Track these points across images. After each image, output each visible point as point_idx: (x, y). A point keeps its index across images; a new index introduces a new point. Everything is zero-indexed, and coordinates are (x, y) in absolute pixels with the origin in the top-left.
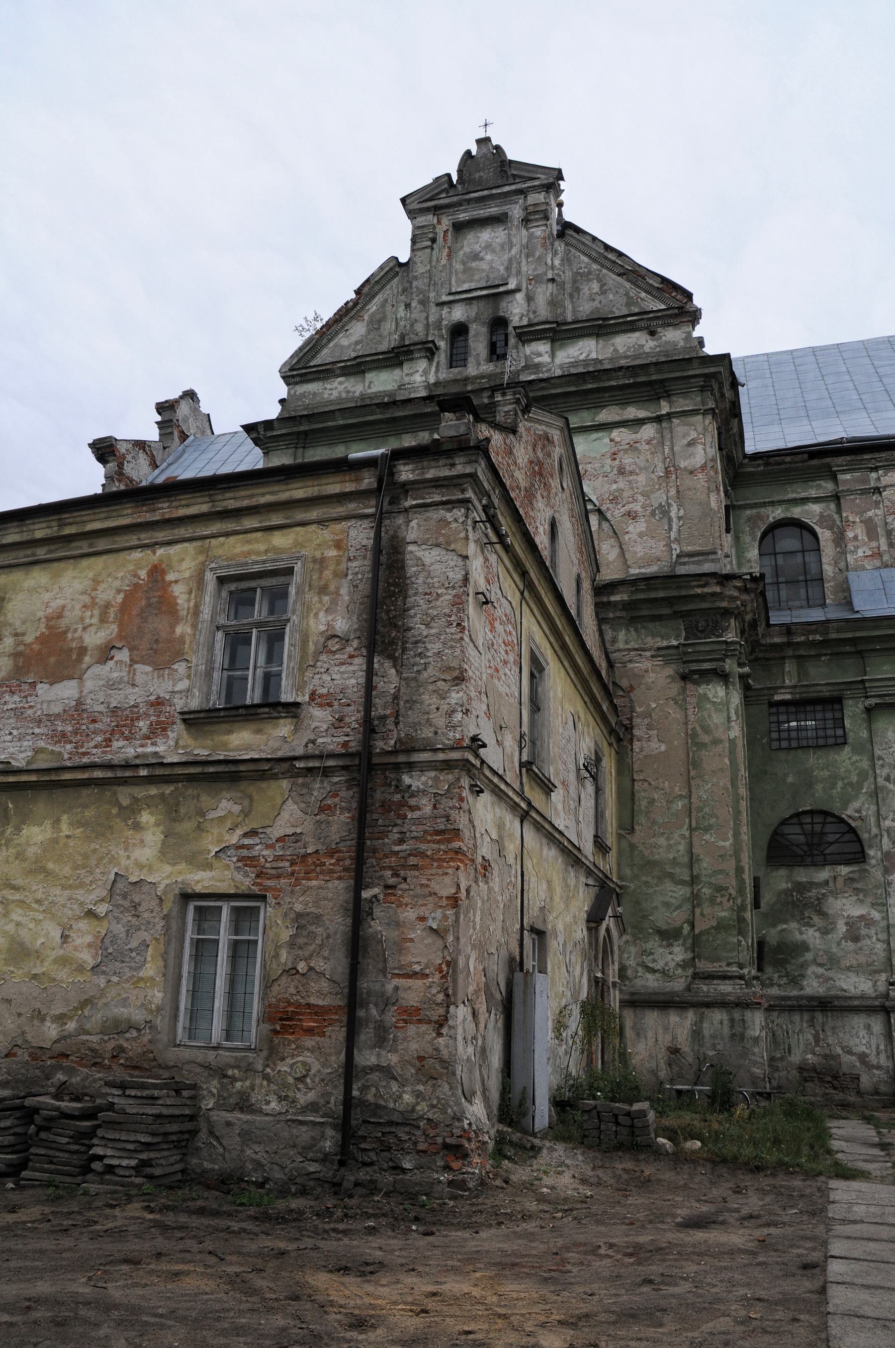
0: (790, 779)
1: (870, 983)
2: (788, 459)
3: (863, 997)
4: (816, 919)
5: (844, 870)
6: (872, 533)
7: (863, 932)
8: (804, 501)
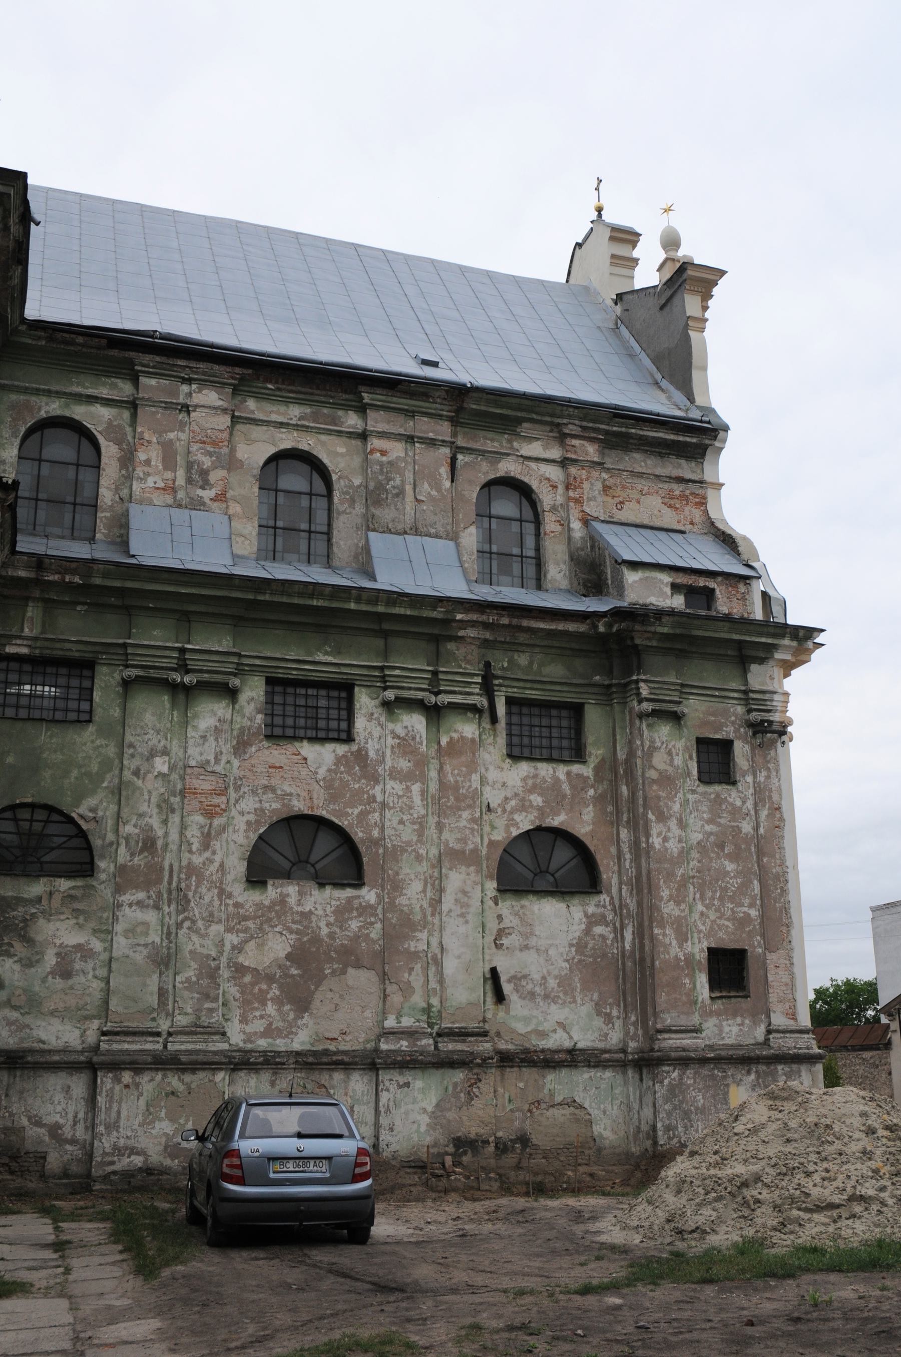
0: (10, 760)
1: (77, 1033)
2: (80, 340)
3: (65, 1051)
4: (19, 948)
5: (64, 884)
6: (169, 462)
7: (78, 965)
8: (92, 399)
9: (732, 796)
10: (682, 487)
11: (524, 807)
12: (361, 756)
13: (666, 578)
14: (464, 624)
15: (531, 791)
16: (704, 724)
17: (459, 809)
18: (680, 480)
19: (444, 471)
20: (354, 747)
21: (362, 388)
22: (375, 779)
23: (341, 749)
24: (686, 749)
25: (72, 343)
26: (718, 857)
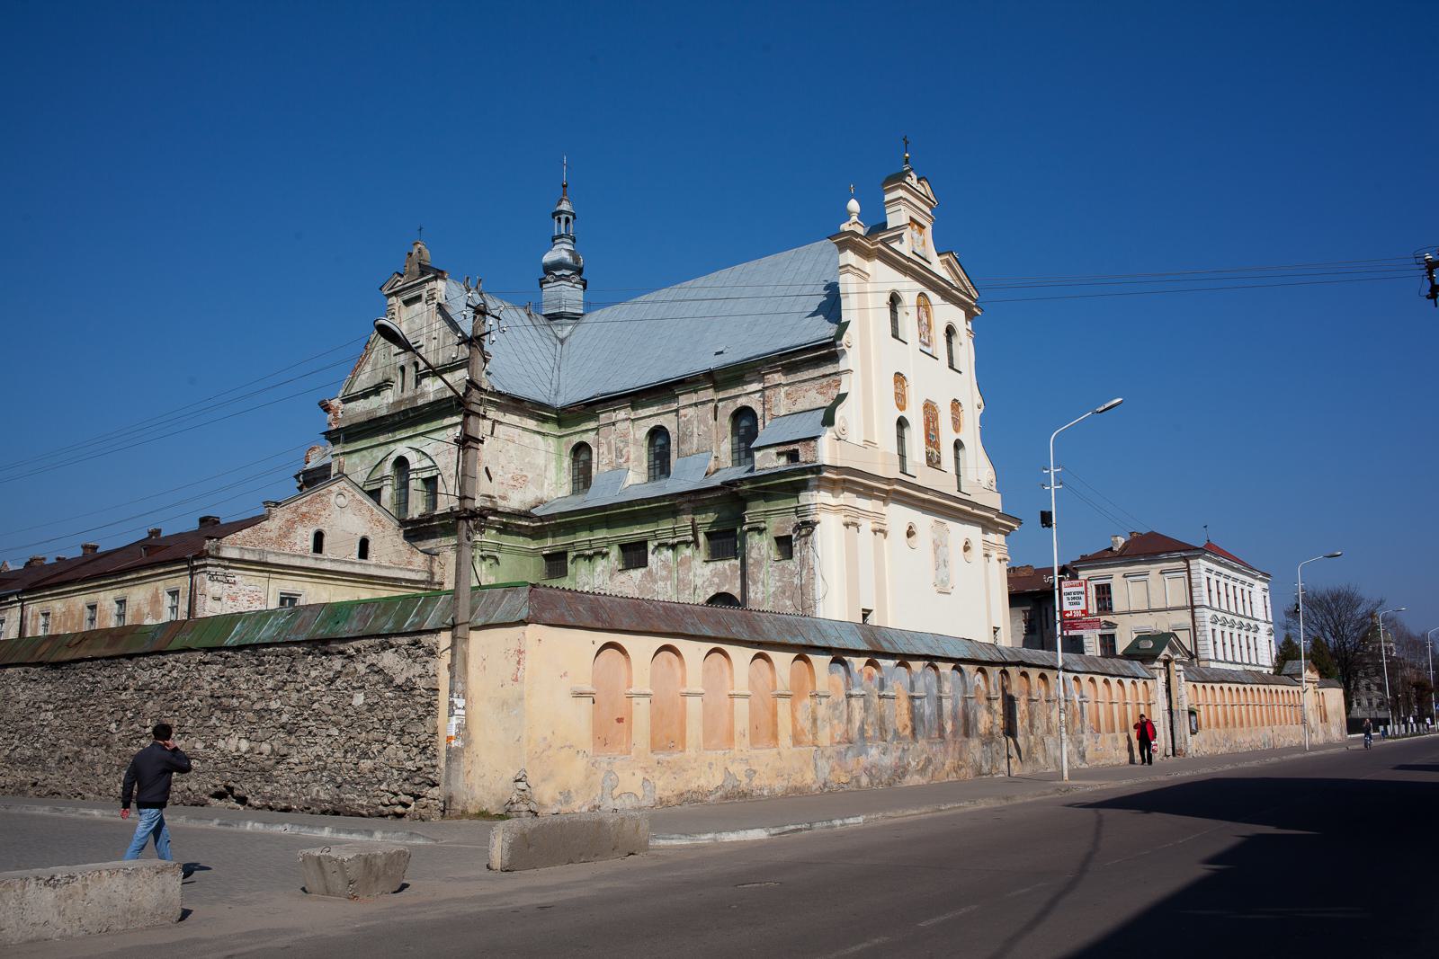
2: (575, 409)
8: (587, 431)
9: (791, 565)
10: (828, 379)
11: (711, 585)
12: (650, 572)
13: (773, 451)
14: (681, 504)
15: (714, 576)
16: (778, 529)
17: (684, 590)
18: (824, 376)
19: (710, 416)
20: (648, 568)
21: (673, 388)
22: (656, 582)
23: (643, 570)
24: (769, 544)
25: (574, 411)
26: (783, 598)
